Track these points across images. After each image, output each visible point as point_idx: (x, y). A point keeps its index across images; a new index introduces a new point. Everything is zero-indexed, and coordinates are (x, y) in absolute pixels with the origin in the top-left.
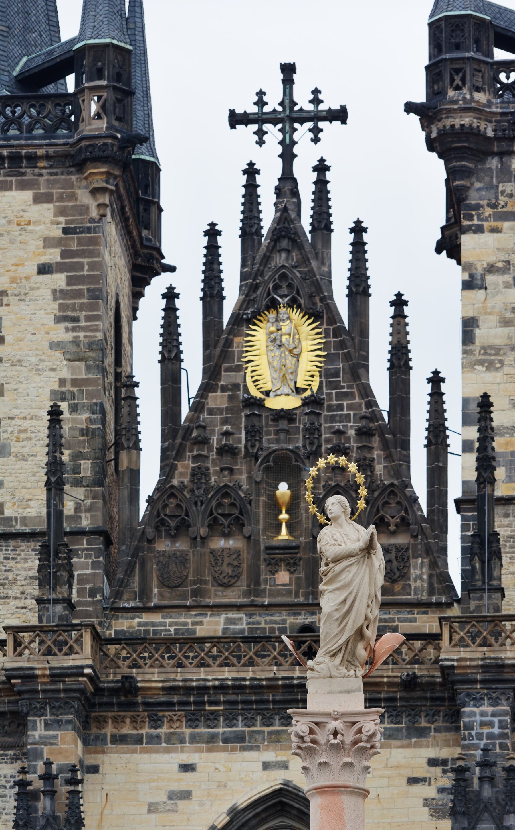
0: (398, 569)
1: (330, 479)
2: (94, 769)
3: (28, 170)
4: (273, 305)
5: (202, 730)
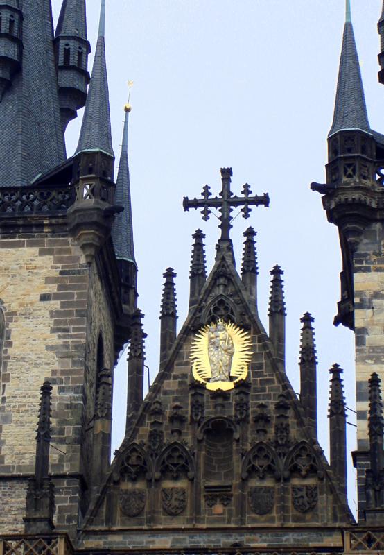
0: (308, 503)
4: (213, 320)
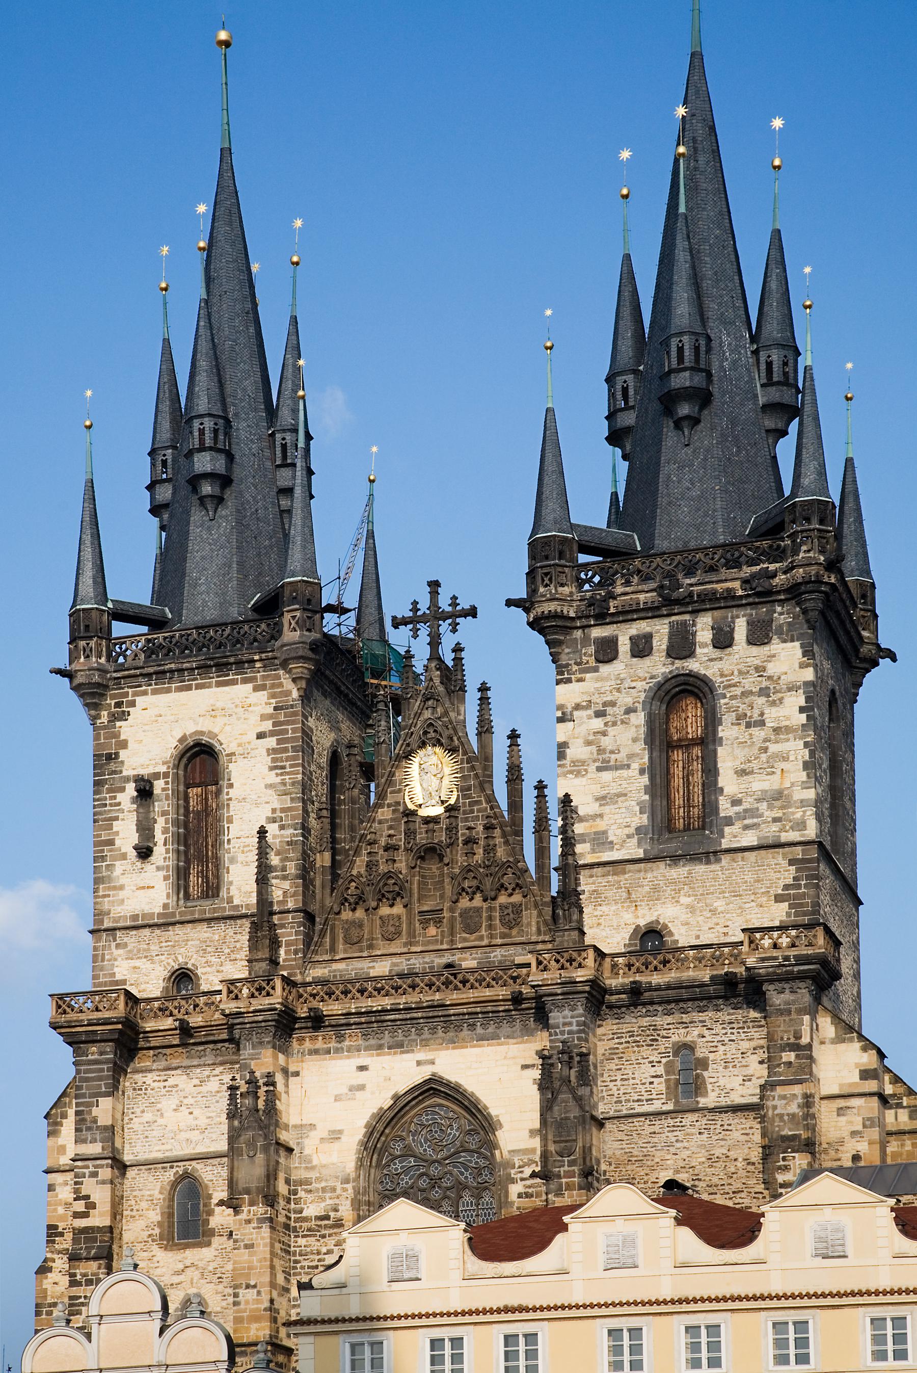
1: (464, 861)
2: (297, 1074)
4: (423, 745)
5: (372, 1042)
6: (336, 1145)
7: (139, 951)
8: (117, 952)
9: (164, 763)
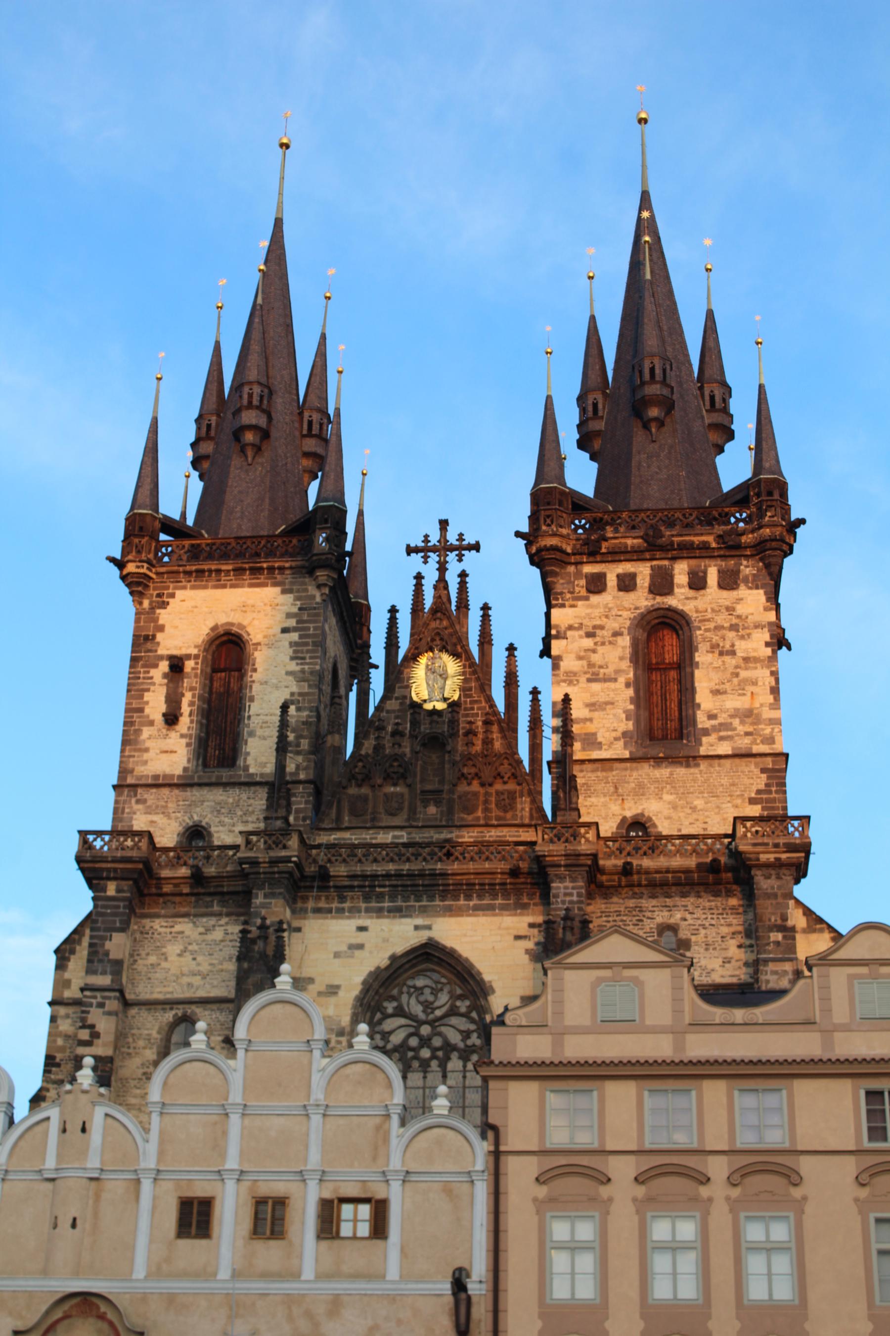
2: (299, 930)
3: (278, 576)
4: (431, 649)
5: (373, 904)
6: (332, 1000)
7: (157, 807)
8: (136, 807)
9: (196, 647)
